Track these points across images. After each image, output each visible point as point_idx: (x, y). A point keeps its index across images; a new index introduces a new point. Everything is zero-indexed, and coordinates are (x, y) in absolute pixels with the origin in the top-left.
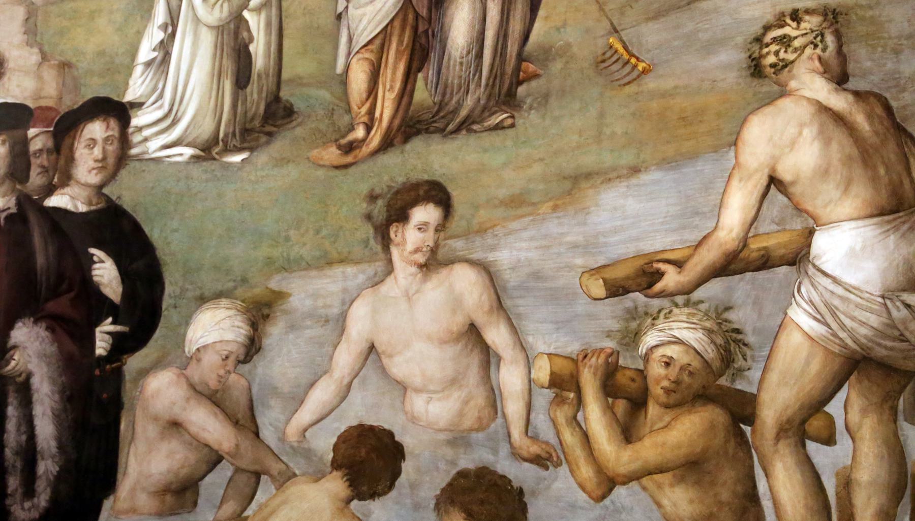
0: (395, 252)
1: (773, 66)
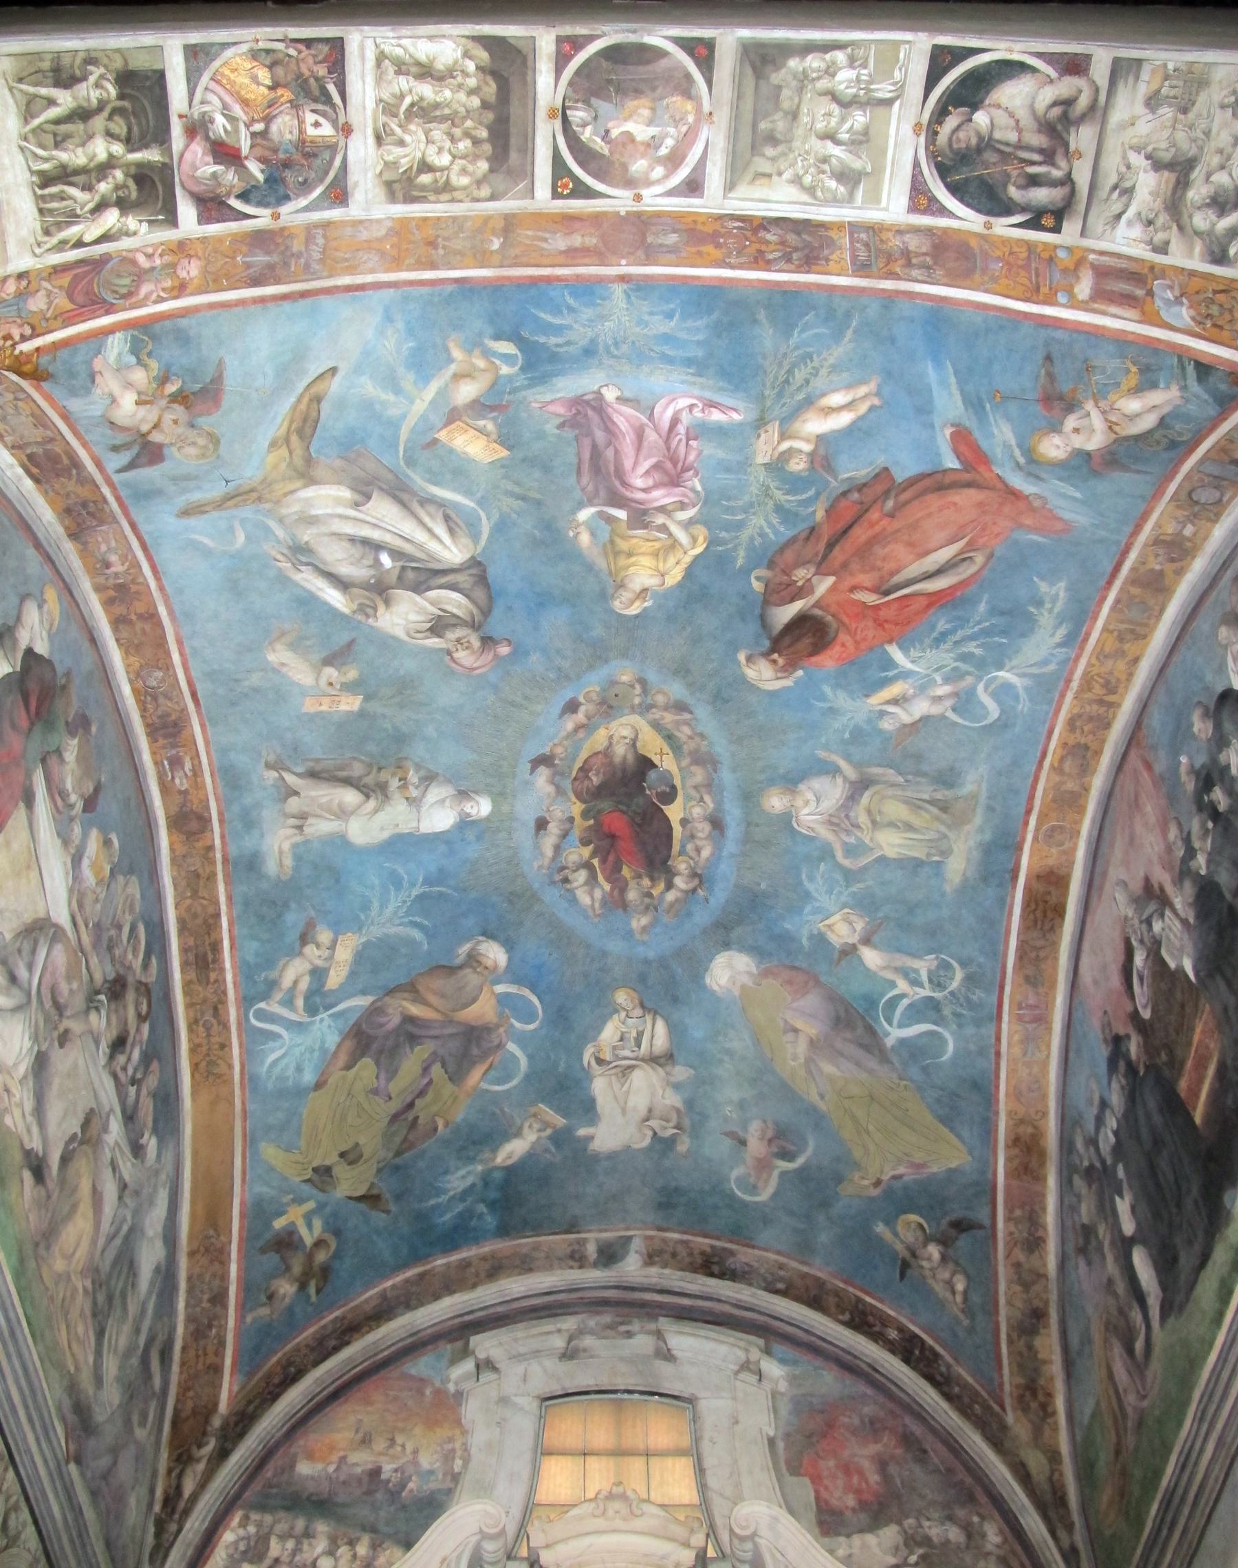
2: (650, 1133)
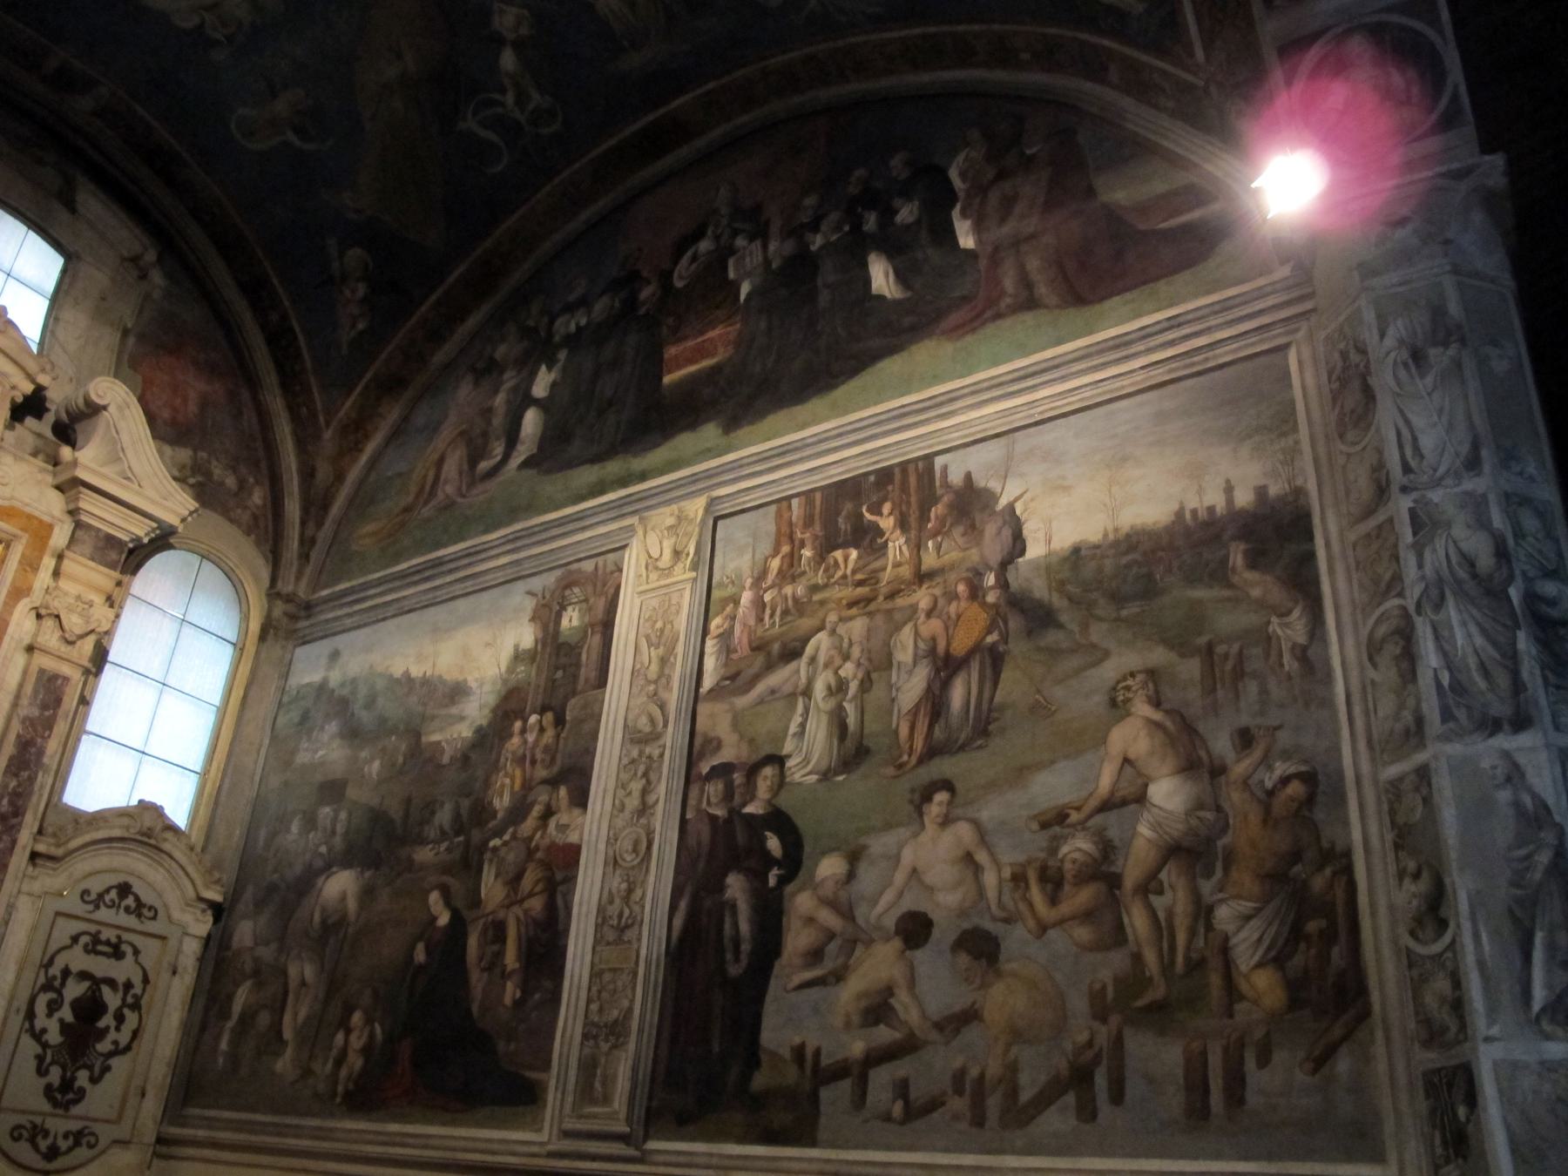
0: (926, 819)
1: (1123, 701)
2: (196, 20)
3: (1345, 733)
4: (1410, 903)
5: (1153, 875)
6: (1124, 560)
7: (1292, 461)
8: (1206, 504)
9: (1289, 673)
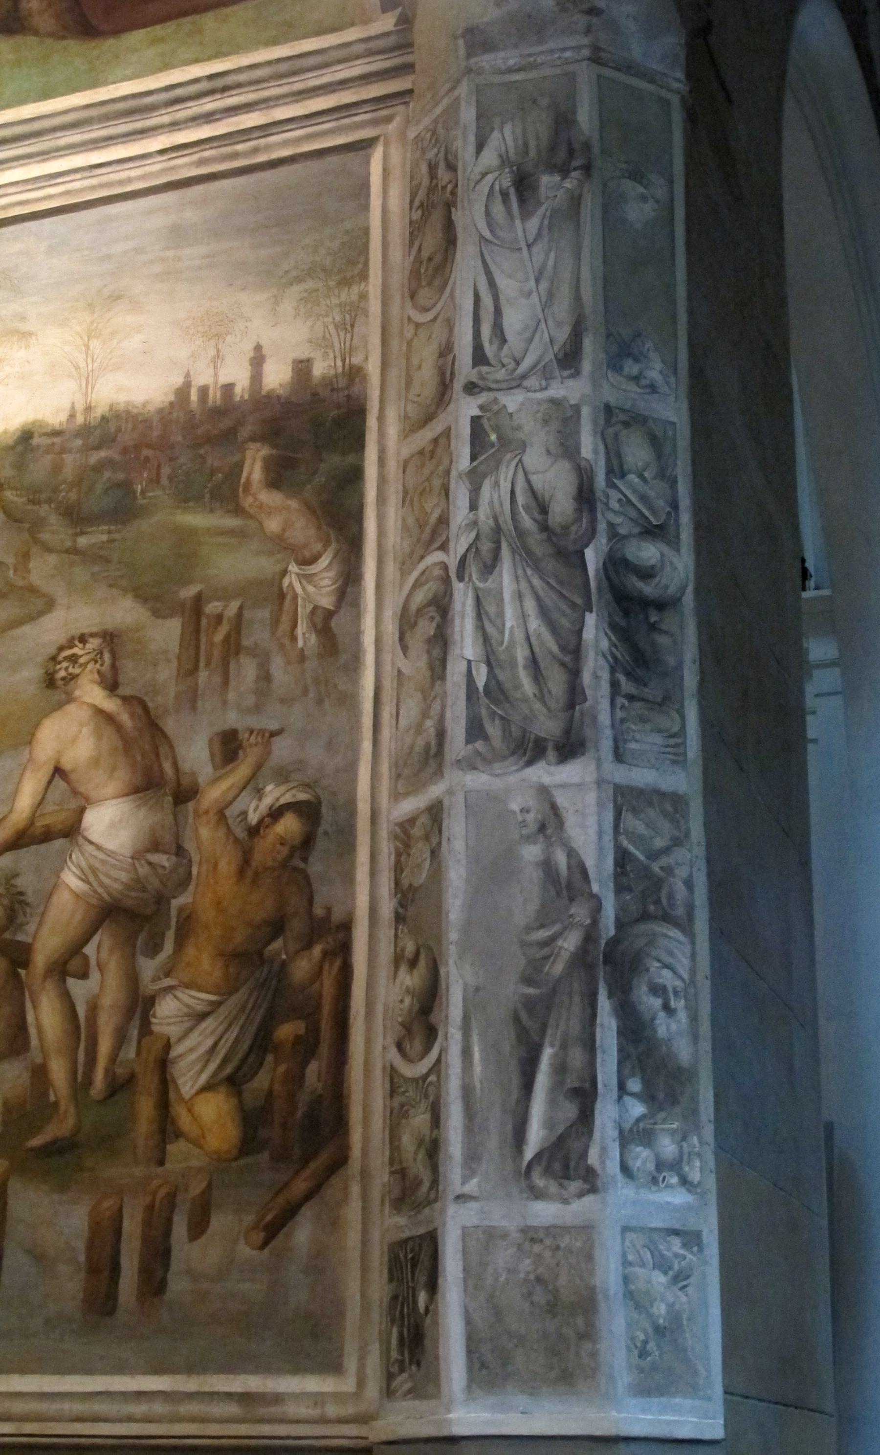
1: (63, 679)
3: (367, 746)
4: (402, 1001)
5: (76, 949)
6: (94, 457)
7: (352, 326)
8: (223, 379)
9: (302, 650)
